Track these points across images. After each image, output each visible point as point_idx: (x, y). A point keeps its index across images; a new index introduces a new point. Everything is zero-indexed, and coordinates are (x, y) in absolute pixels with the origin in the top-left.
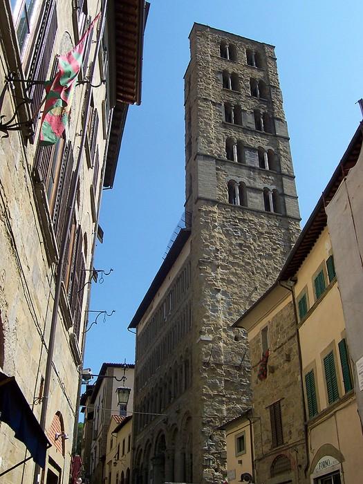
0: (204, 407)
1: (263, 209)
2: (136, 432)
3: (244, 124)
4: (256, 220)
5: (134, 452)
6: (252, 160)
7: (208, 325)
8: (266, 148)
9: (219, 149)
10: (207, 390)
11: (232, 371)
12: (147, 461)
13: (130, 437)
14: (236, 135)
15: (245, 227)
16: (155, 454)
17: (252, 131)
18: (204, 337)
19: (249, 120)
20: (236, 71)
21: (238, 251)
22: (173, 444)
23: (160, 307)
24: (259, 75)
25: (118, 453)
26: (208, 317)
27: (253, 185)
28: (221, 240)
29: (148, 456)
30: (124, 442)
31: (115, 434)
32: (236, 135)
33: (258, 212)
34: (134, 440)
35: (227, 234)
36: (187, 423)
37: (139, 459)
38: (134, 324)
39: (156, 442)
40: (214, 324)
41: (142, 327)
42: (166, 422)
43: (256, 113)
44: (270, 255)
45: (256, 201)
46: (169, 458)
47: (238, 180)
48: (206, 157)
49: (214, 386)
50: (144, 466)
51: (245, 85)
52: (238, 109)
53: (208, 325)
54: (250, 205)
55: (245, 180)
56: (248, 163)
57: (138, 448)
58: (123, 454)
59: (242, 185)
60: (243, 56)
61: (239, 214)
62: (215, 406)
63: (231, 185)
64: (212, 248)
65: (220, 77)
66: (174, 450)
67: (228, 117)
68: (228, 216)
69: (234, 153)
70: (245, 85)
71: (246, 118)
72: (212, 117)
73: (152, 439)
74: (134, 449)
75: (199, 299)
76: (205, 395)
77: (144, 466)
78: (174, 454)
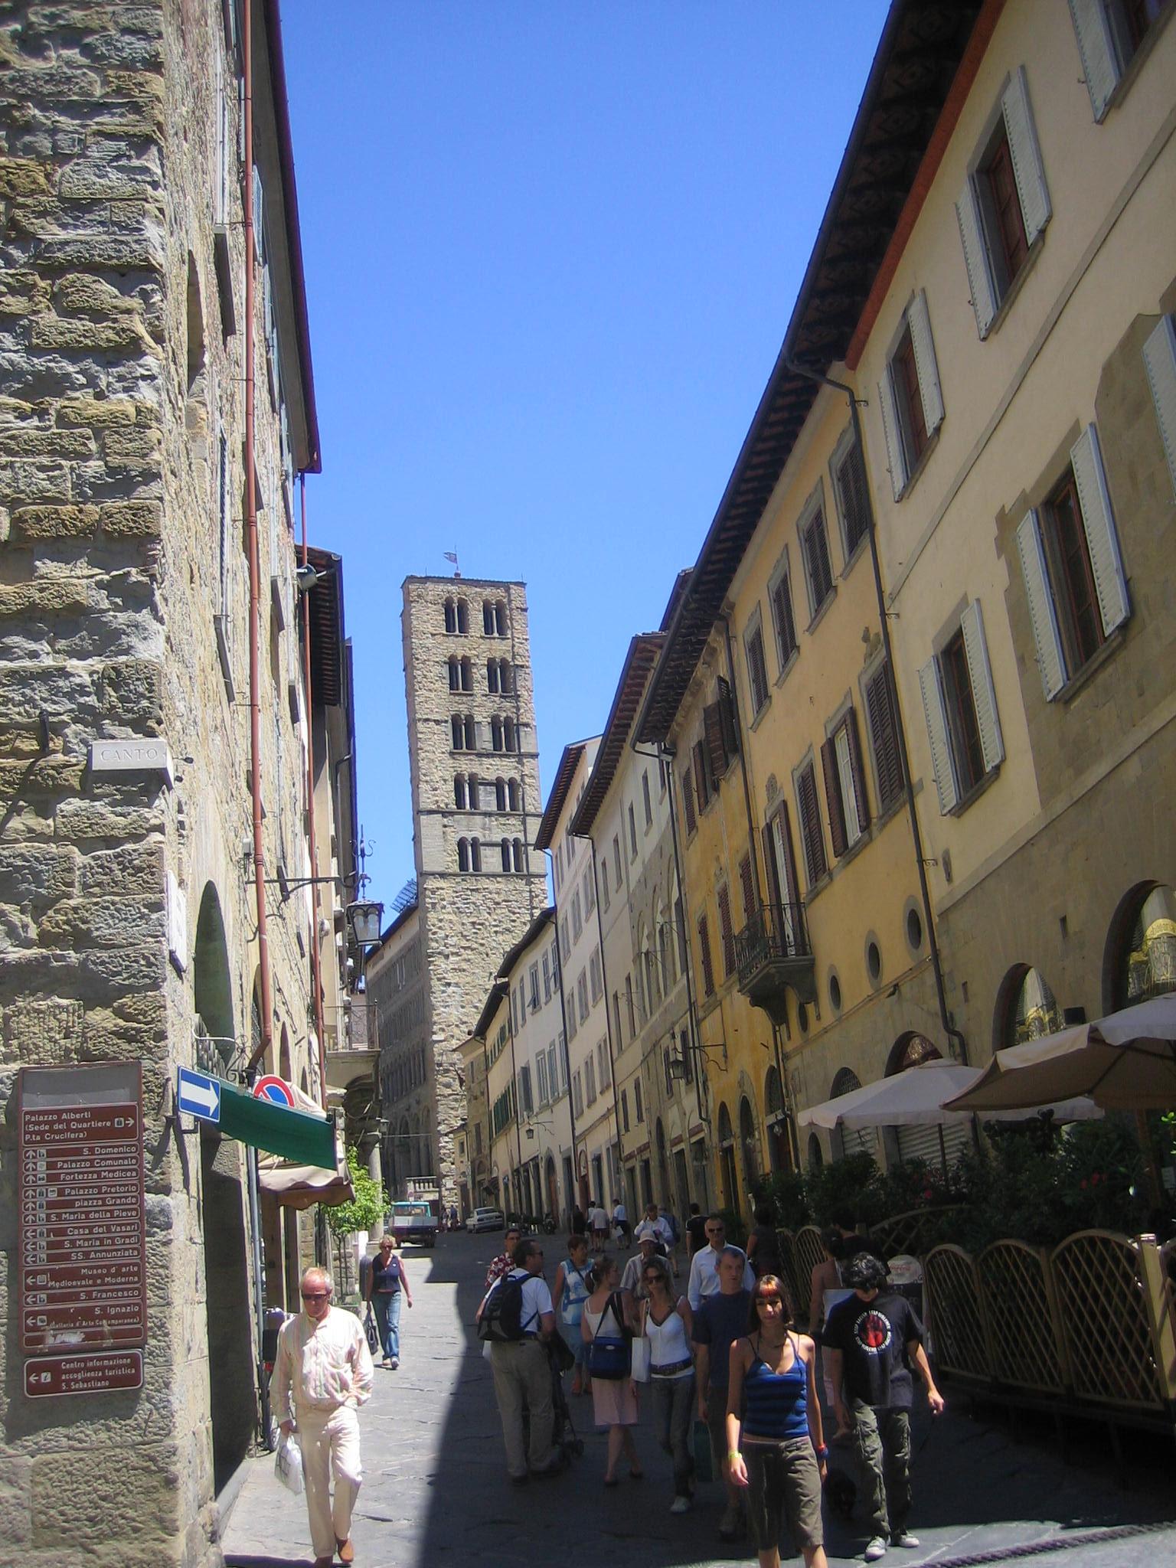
1: (500, 869)
3: (478, 745)
4: (491, 887)
6: (487, 799)
8: (506, 777)
9: (446, 796)
14: (468, 766)
15: (476, 898)
17: (488, 756)
18: (435, 1038)
19: (484, 738)
20: (468, 653)
21: (469, 931)
24: (499, 648)
27: (488, 839)
28: (451, 922)
32: (468, 766)
33: (495, 876)
35: (459, 911)
43: (495, 724)
44: (508, 930)
45: (492, 860)
47: (469, 836)
48: (431, 812)
49: (448, 1086)
51: (480, 673)
52: (470, 722)
54: (485, 869)
55: (477, 833)
56: (483, 808)
59: (475, 840)
60: (476, 618)
61: (471, 883)
63: (462, 844)
64: (441, 934)
65: (445, 671)
67: (457, 744)
68: (459, 888)
69: (465, 788)
70: (480, 673)
71: (481, 735)
72: (437, 741)
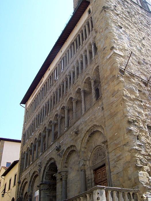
0: (126, 107)
2: (21, 171)
5: (19, 186)
7: (118, 45)
10: (126, 92)
11: (143, 85)
12: (32, 190)
13: (16, 175)
16: (42, 181)
22: (66, 167)
23: (51, 77)
25: (5, 189)
26: (117, 40)
29: (32, 186)
30: (10, 180)
31: (3, 177)
34: (20, 177)
36: (88, 141)
37: (23, 190)
38: (24, 101)
39: (44, 171)
40: (122, 46)
41: (30, 102)
42: (58, 149)
46: (61, 179)
50: (29, 194)
53: (118, 45)
57: (23, 181)
58: (9, 188)
62: (136, 108)
66: (67, 172)
73: (40, 170)
74: (19, 183)
75: (107, 28)
76: (126, 96)
77: (29, 194)
78: (67, 176)
